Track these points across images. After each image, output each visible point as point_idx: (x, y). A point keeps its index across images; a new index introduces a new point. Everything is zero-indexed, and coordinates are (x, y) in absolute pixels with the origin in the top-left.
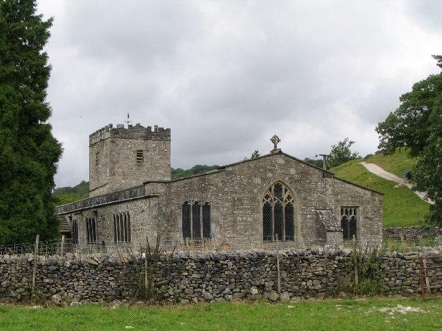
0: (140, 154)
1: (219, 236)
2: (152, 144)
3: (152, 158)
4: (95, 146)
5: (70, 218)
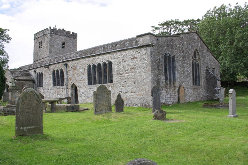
0: (63, 43)
1: (179, 80)
2: (69, 39)
4: (39, 38)
5: (35, 71)
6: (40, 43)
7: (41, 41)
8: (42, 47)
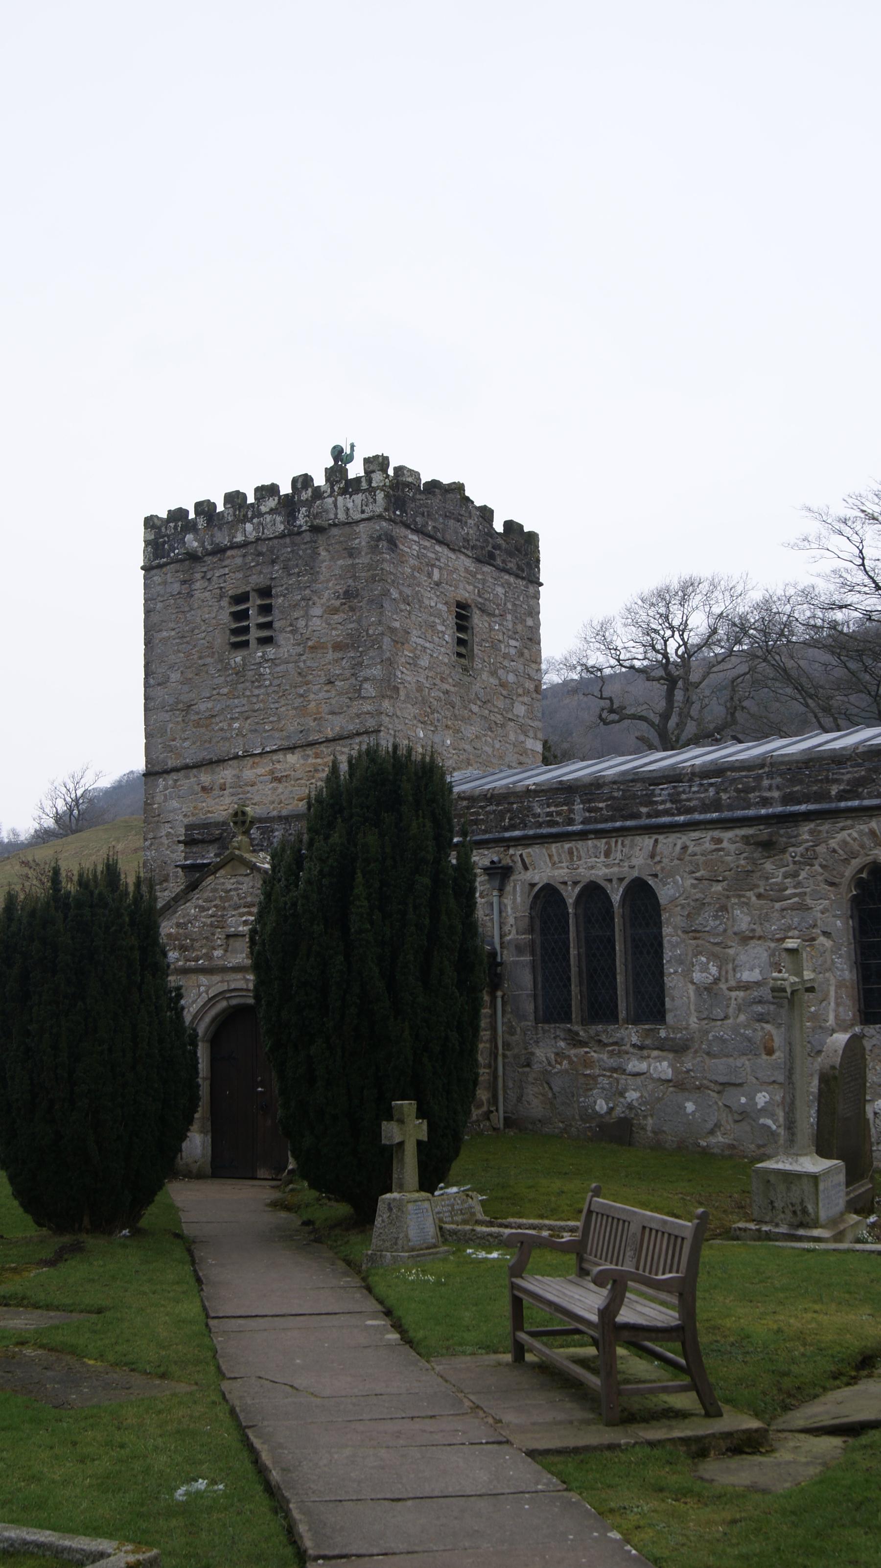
0: (462, 615)
3: (494, 647)
6: (242, 598)
7: (257, 580)
8: (281, 638)
